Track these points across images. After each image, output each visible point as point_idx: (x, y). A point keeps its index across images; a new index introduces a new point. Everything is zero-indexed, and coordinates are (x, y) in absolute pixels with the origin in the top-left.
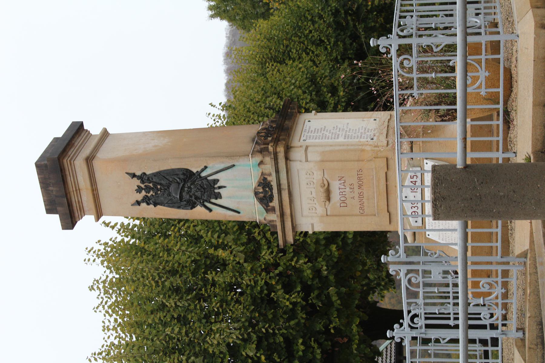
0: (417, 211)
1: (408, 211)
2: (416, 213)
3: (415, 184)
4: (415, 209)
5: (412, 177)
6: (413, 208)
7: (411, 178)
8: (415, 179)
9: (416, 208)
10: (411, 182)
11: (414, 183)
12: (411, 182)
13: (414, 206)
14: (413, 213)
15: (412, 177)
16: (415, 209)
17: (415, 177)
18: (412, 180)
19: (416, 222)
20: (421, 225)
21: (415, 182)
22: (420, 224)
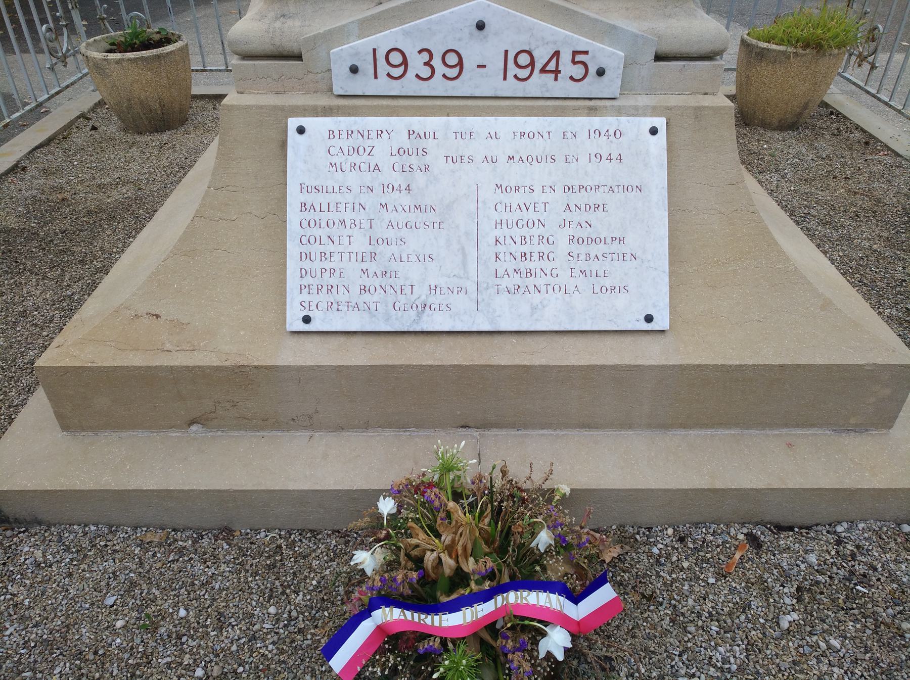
0: (411, 74)
1: (406, 33)
2: (397, 72)
3: (543, 70)
4: (417, 64)
5: (579, 58)
6: (425, 57)
7: (575, 53)
8: (567, 68)
9: (425, 72)
10: (557, 54)
11: (552, 66)
12: (557, 54)
13: (437, 62)
14: (396, 58)
15: (579, 58)
16: (417, 64)
17: (578, 71)
18: (566, 57)
19: (354, 70)
20: (337, 90)
21: (557, 72)
22: (342, 83)
